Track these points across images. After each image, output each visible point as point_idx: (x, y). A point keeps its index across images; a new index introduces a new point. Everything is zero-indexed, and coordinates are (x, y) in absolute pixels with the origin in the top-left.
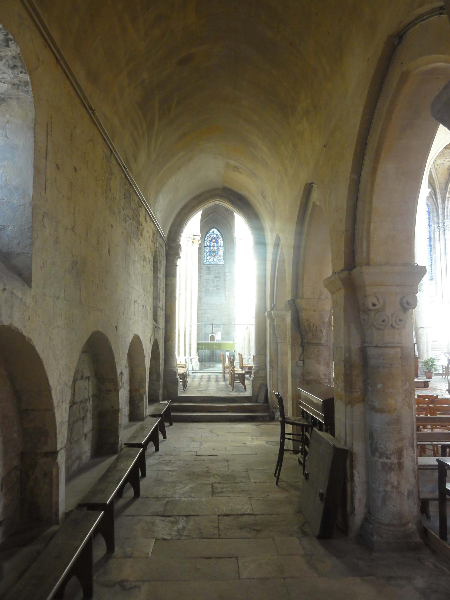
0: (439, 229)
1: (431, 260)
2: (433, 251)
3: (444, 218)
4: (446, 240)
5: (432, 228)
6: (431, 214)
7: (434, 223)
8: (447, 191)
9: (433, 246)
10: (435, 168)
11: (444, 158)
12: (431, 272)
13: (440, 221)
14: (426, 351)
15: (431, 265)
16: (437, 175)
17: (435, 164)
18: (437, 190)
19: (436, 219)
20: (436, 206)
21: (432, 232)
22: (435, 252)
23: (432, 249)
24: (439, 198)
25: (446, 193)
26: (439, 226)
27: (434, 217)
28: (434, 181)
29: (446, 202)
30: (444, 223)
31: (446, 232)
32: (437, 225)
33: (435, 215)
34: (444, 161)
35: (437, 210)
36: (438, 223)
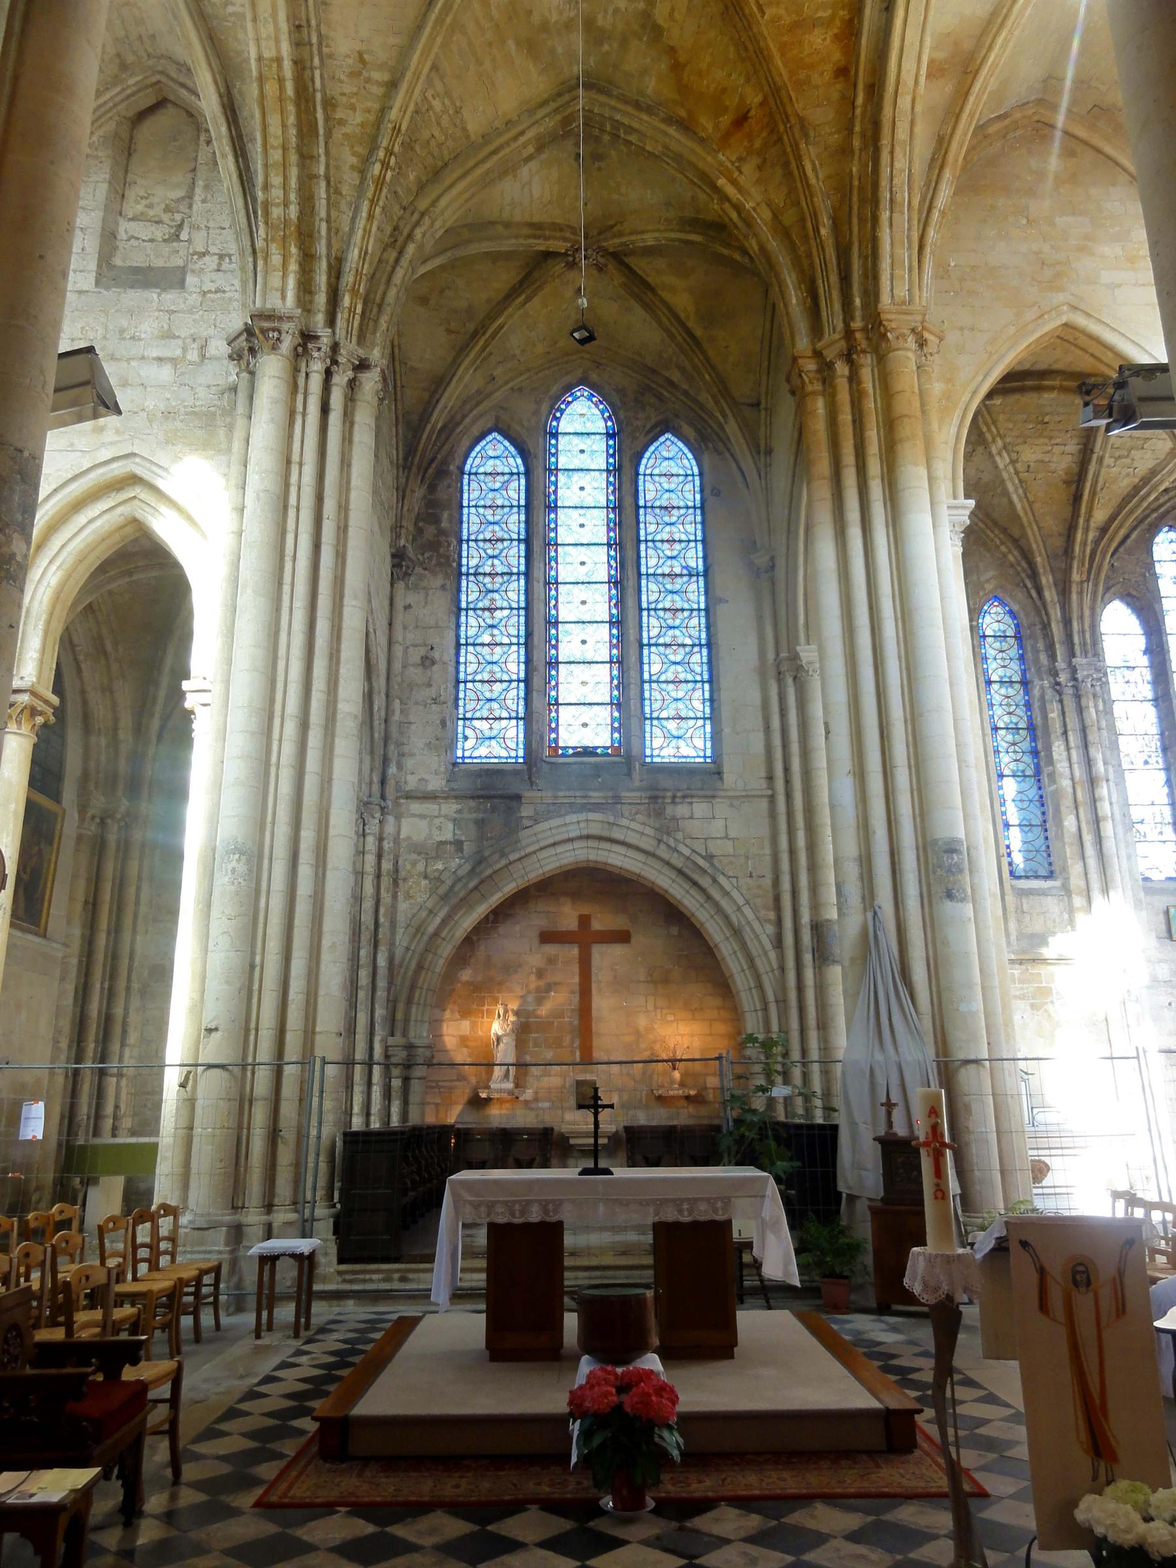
0: (1060, 693)
1: (1043, 805)
2: (1046, 770)
3: (1072, 654)
4: (1088, 732)
5: (1036, 692)
6: (1028, 645)
7: (1038, 671)
8: (1072, 558)
9: (1042, 754)
10: (1021, 481)
11: (1046, 441)
12: (1044, 848)
13: (1061, 664)
14: (997, 1177)
15: (1045, 821)
16: (1030, 504)
17: (1018, 466)
18: (1039, 559)
19: (1043, 658)
20: (1040, 616)
21: (1036, 705)
22: (1052, 777)
23: (1042, 764)
24: (1049, 587)
25: (1071, 567)
26: (1058, 684)
27: (1038, 652)
28: (1022, 526)
29: (1074, 596)
30: (1073, 670)
31: (1084, 702)
32: (1051, 679)
33: (1041, 645)
34: (1048, 452)
35: (1046, 626)
36: (1054, 673)
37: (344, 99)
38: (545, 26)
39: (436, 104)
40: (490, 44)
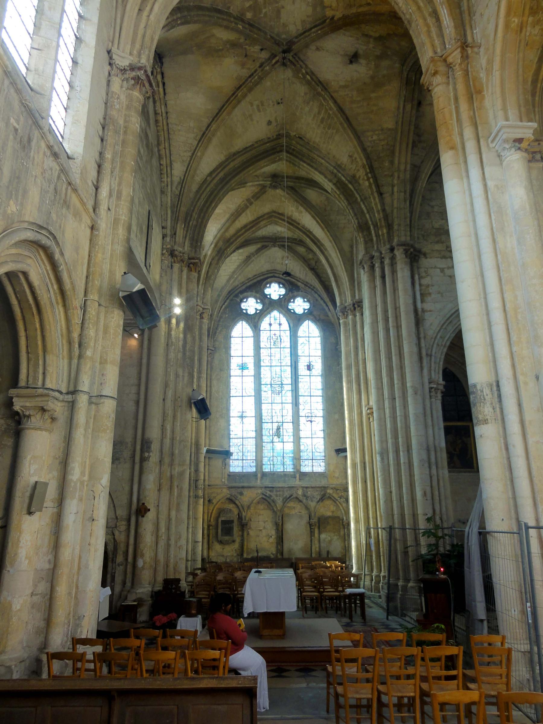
37: (356, 171)
38: (372, 78)
39: (375, 137)
40: (368, 105)
